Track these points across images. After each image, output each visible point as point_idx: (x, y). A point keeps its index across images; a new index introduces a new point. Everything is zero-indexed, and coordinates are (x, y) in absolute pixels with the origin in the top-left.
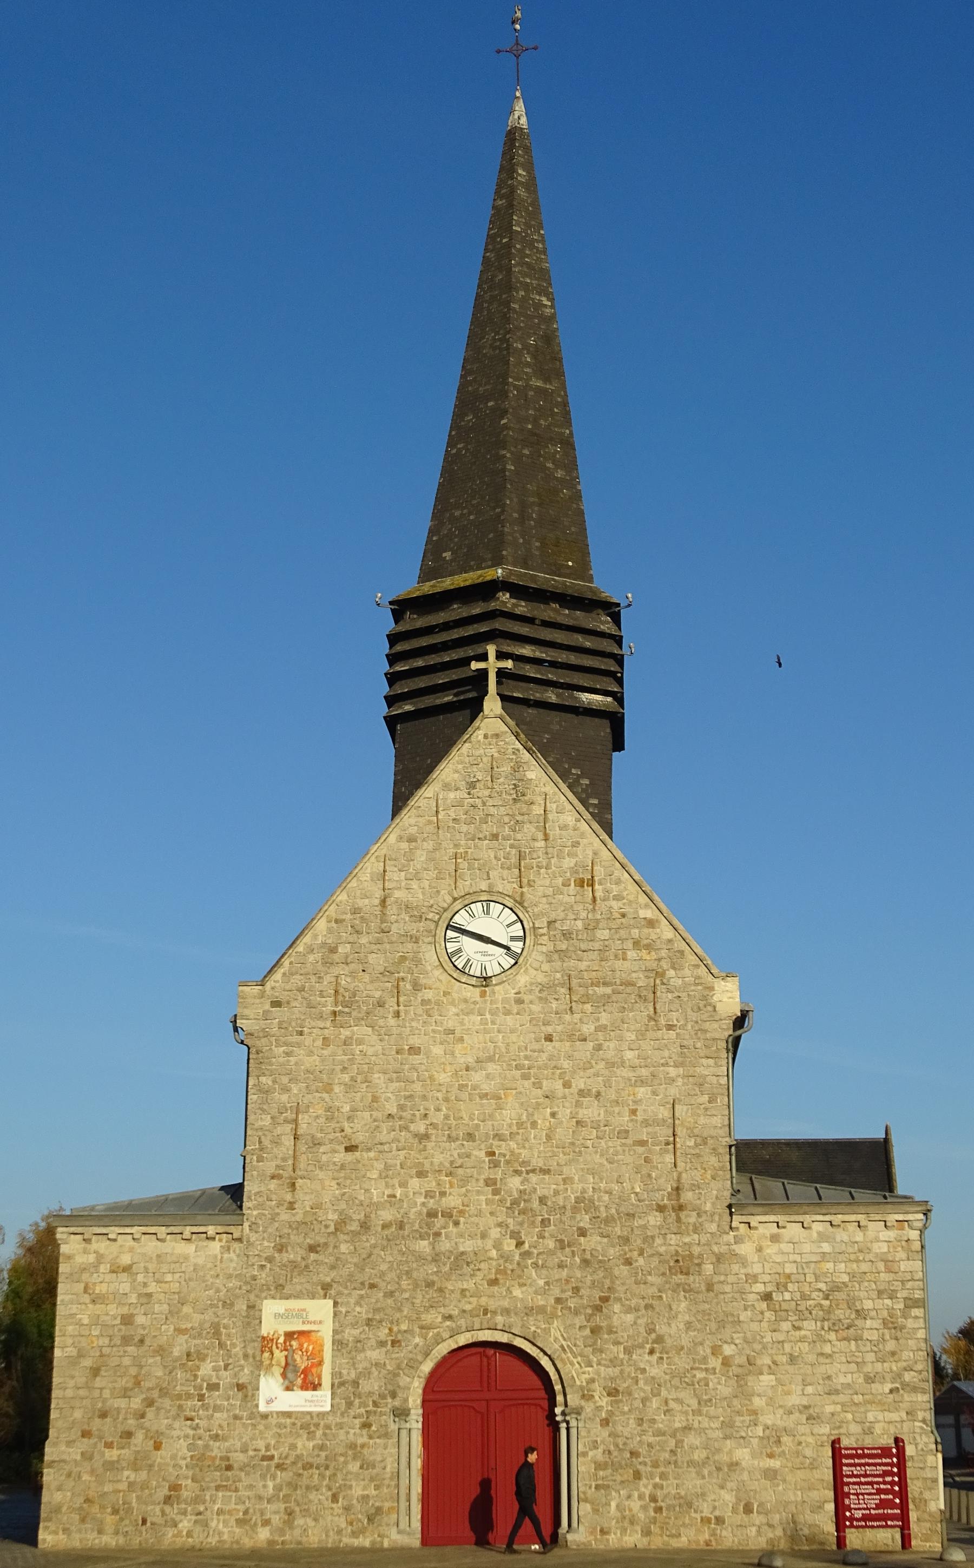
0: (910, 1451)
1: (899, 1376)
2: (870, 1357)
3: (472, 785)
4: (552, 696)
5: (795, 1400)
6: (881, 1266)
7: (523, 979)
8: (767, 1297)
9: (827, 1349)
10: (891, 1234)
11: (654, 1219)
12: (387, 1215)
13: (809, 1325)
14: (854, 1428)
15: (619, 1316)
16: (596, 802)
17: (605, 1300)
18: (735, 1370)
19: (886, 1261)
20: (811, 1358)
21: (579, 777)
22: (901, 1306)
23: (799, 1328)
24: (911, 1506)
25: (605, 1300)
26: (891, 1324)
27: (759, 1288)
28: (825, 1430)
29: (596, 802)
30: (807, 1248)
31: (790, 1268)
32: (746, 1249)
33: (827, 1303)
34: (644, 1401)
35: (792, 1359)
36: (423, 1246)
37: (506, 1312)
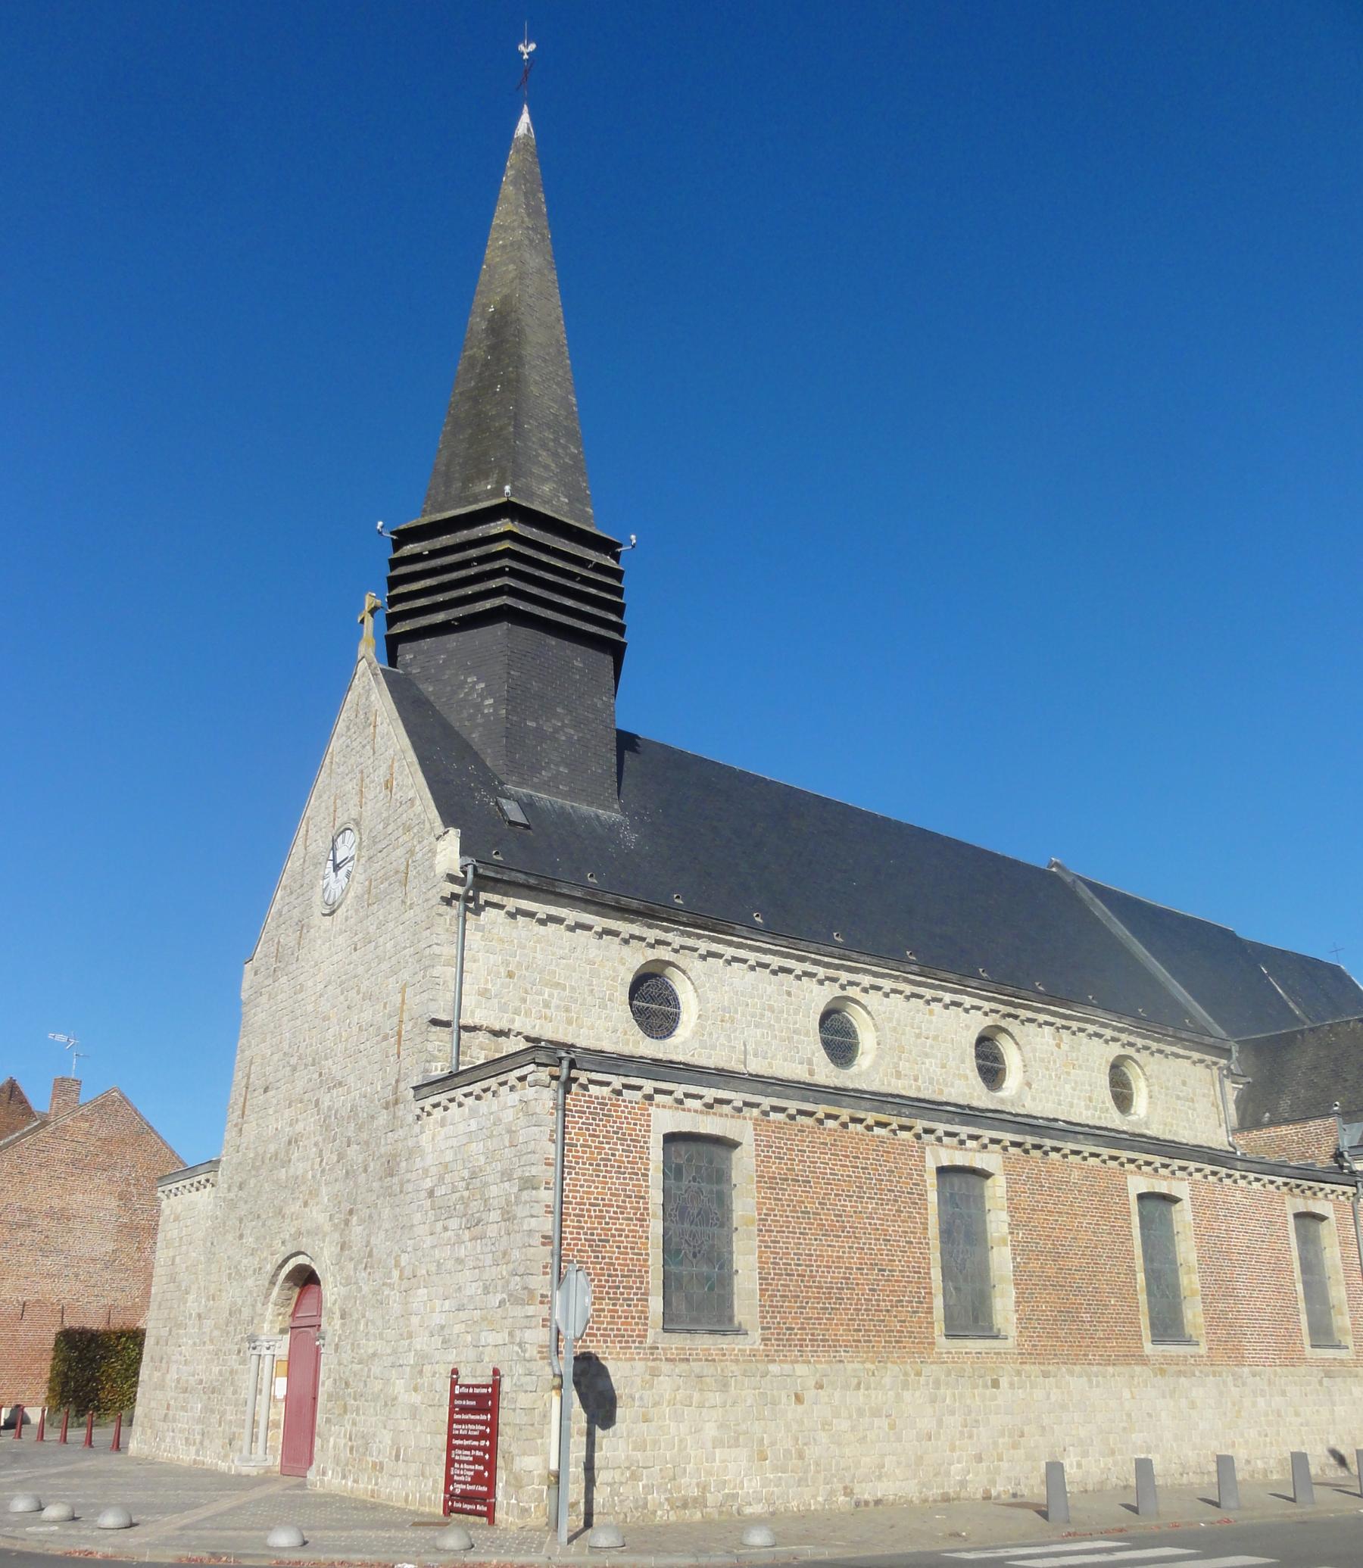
0: (506, 1386)
1: (508, 1282)
2: (488, 1260)
3: (348, 729)
4: (440, 617)
5: (437, 1319)
6: (506, 1137)
7: (351, 894)
8: (431, 1193)
9: (462, 1253)
10: (515, 1097)
11: (383, 1118)
12: (272, 1148)
13: (454, 1223)
14: (471, 1354)
15: (357, 1231)
16: (491, 701)
17: (351, 1212)
18: (405, 1284)
19: (510, 1131)
20: (450, 1265)
21: (475, 683)
22: (515, 1189)
23: (446, 1229)
24: (500, 1462)
25: (351, 1212)
26: (508, 1217)
27: (428, 1183)
28: (452, 1356)
29: (491, 701)
30: (462, 1128)
31: (449, 1156)
32: (425, 1139)
33: (466, 1194)
34: (358, 1321)
35: (439, 1265)
36: (282, 1174)
37: (308, 1232)
